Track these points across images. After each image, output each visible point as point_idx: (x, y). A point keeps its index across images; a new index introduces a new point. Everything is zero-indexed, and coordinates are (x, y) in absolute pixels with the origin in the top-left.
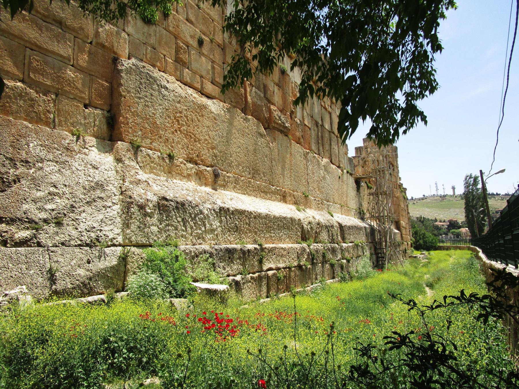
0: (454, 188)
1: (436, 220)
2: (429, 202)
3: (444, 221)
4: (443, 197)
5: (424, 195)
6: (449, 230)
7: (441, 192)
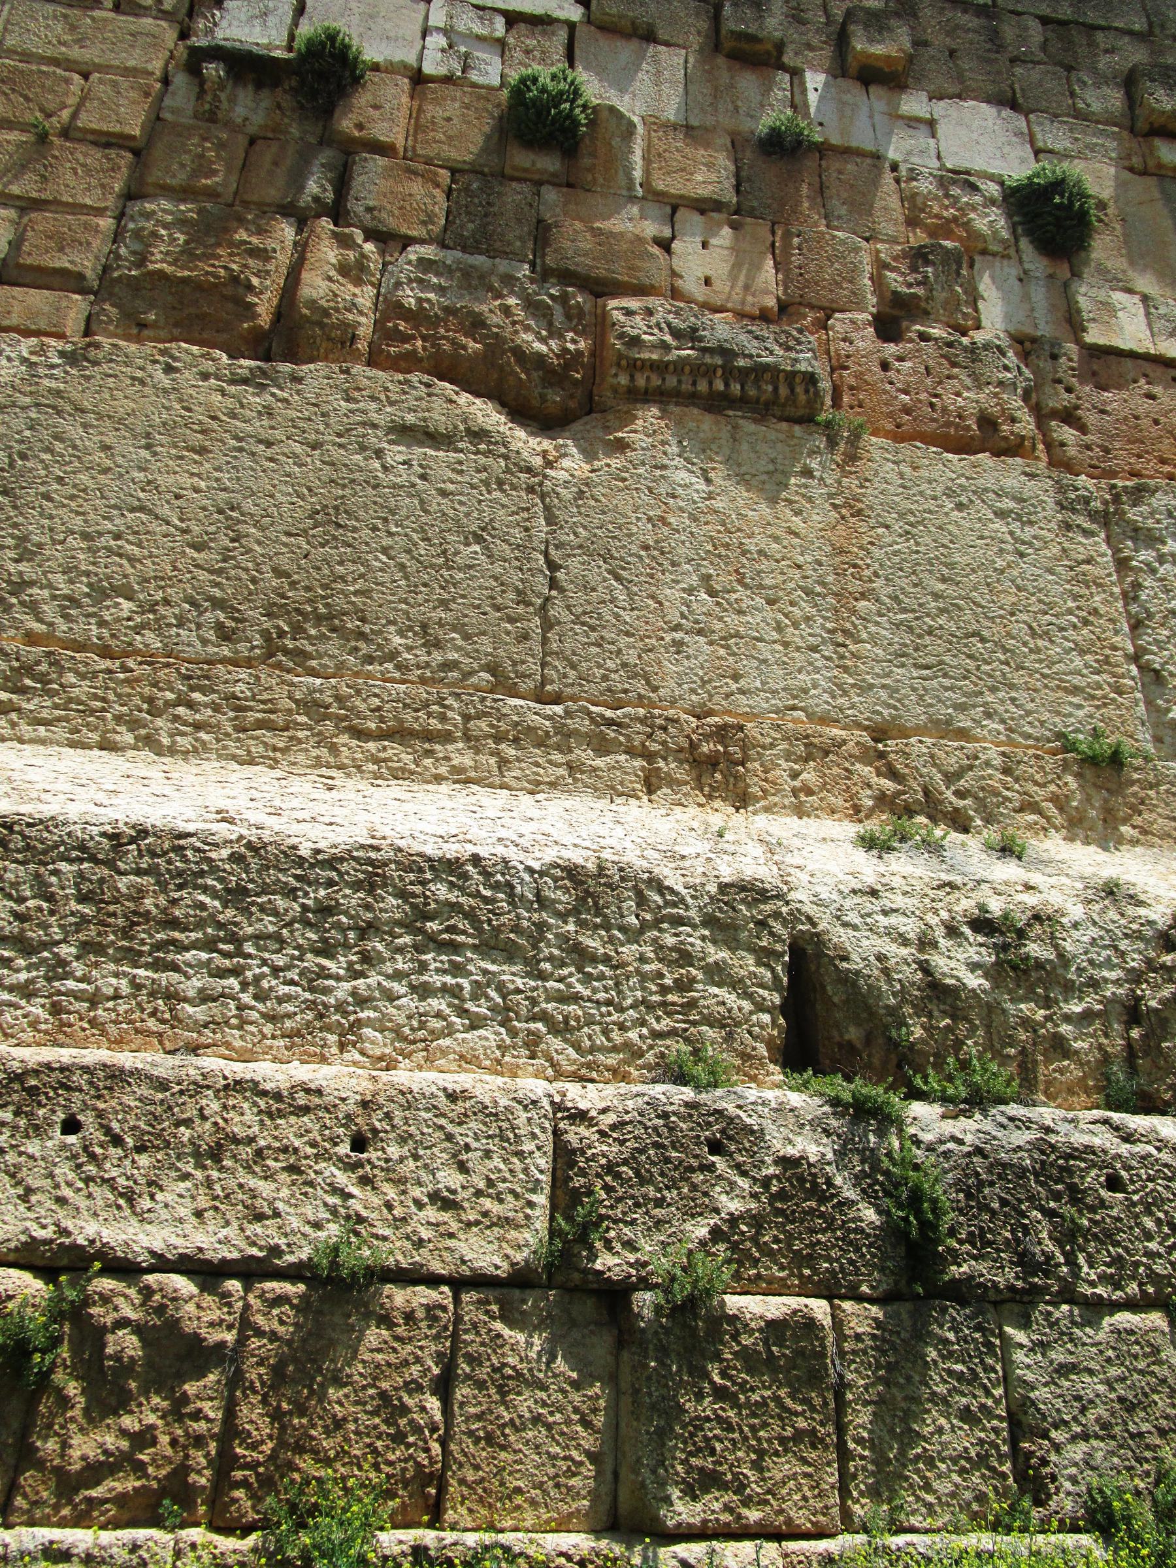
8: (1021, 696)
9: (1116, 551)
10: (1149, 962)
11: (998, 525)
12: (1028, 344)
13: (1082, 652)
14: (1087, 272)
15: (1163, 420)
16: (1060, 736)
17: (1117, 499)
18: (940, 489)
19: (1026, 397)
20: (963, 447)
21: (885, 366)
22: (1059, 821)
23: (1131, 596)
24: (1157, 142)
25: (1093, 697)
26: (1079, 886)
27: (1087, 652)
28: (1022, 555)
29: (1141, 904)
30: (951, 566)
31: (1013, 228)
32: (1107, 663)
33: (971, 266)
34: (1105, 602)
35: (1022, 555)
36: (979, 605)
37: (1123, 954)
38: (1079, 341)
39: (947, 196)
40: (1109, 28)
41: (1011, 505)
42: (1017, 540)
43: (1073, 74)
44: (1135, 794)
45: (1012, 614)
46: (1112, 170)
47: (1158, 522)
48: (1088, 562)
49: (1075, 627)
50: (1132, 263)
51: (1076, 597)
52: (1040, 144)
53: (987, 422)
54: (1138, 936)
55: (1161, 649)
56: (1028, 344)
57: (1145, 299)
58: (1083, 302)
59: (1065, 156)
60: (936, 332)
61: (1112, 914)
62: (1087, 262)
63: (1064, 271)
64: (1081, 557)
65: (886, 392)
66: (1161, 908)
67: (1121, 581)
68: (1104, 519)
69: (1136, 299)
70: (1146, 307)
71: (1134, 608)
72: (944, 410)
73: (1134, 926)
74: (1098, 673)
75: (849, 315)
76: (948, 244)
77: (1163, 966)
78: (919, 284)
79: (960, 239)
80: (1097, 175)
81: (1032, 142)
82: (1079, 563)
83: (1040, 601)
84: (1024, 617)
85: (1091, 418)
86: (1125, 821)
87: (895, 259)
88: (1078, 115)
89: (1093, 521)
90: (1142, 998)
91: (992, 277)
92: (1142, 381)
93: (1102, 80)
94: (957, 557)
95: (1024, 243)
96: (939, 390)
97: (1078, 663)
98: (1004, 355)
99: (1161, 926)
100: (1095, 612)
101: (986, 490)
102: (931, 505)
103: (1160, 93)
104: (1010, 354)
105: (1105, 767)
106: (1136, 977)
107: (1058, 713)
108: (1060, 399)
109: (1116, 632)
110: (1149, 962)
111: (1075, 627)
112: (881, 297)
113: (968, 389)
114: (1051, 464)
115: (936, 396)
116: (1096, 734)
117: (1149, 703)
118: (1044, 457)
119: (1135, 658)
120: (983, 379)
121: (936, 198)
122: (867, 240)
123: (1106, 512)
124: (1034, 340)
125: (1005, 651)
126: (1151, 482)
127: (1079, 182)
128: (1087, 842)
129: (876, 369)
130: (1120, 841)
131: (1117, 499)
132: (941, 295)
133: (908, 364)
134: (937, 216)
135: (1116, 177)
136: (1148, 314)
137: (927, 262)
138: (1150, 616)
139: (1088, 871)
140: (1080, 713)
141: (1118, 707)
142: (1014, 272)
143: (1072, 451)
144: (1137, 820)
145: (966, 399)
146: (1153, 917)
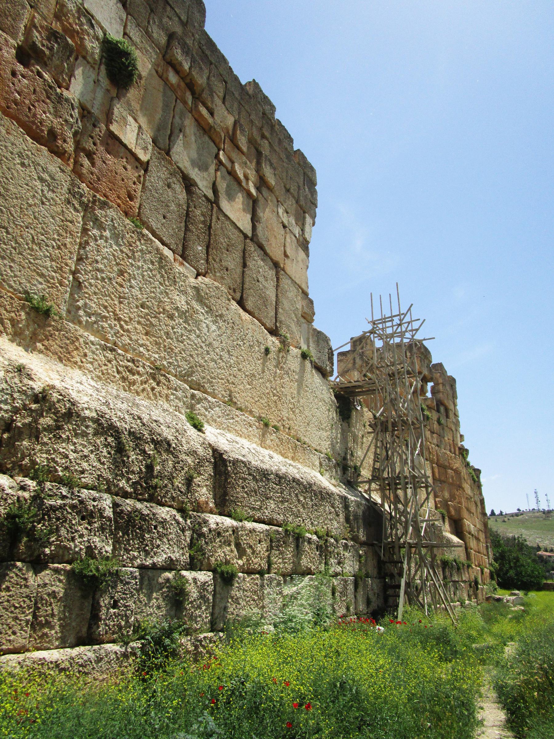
2: (526, 520)
5: (519, 510)
7: (544, 506)
8: (16, 267)
9: (85, 224)
10: (25, 406)
11: (38, 183)
12: (86, 112)
13: (52, 260)
14: (123, 100)
15: (126, 180)
16: (26, 292)
17: (94, 202)
18: (16, 151)
19: (75, 134)
20: (37, 138)
21: (14, 74)
22: (10, 330)
23: (83, 246)
24: (170, 69)
25: (49, 282)
26: (7, 363)
27: (54, 261)
28: (43, 203)
29: (31, 379)
30: (7, 190)
31: (102, 57)
32: (61, 270)
33: (76, 59)
34: (71, 243)
35: (43, 203)
36: (12, 215)
37: (14, 399)
38: (107, 127)
39: (79, 19)
40: (173, 9)
41: (48, 178)
42: (44, 195)
43: (152, 14)
44: (49, 331)
45: (27, 228)
46: (150, 66)
47: (106, 221)
48: (71, 222)
49: (53, 247)
50: (141, 109)
51: (59, 235)
52: (128, 32)
53: (52, 133)
54: (24, 393)
55: (86, 274)
56: (86, 112)
57: (140, 127)
58: (116, 111)
59: (134, 44)
60: (46, 76)
61: (17, 380)
62: (125, 96)
63: (114, 93)
64: (69, 218)
65: (9, 87)
66: (39, 384)
67: (81, 238)
68: (86, 207)
69: (137, 125)
70: (139, 131)
71: (82, 252)
72: (35, 115)
73: (24, 388)
74: (55, 272)
75: (4, 35)
76: (69, 40)
77: (30, 409)
78: (48, 48)
79: (76, 43)
80: (144, 63)
81: (125, 27)
82: (67, 221)
83: (43, 228)
84: (32, 232)
85: (99, 162)
86: (41, 341)
87: (42, 27)
88: (147, 32)
89: (80, 206)
90: (15, 420)
91: (83, 72)
92: (125, 160)
93: (162, 26)
94: (11, 187)
95: (103, 67)
96: (36, 104)
97: (48, 264)
98: (73, 109)
99: (36, 391)
100: (65, 244)
101: (39, 164)
102: (8, 155)
103: (179, 51)
104: (76, 111)
105: (41, 314)
106: (16, 411)
107: (30, 282)
108: (89, 145)
109: (70, 258)
110: (25, 406)
111: (53, 247)
112: (26, 39)
113: (50, 113)
114: (73, 171)
115: (33, 106)
116: (43, 298)
117: (72, 294)
118: (72, 165)
119: (74, 273)
120: (59, 114)
121: (73, 15)
122: (32, 7)
123: (87, 205)
124: (89, 112)
125: (16, 242)
126: (111, 203)
127: (135, 60)
128: (19, 345)
129: (9, 72)
130: (34, 349)
131: (94, 202)
132: (56, 61)
133: (26, 81)
134: (70, 24)
135: (150, 71)
136: (138, 134)
137: (57, 42)
138: (87, 258)
139: (14, 358)
140: (40, 286)
141: (58, 291)
142: (94, 76)
143: (84, 171)
144: (46, 343)
145: (47, 117)
146: (34, 386)
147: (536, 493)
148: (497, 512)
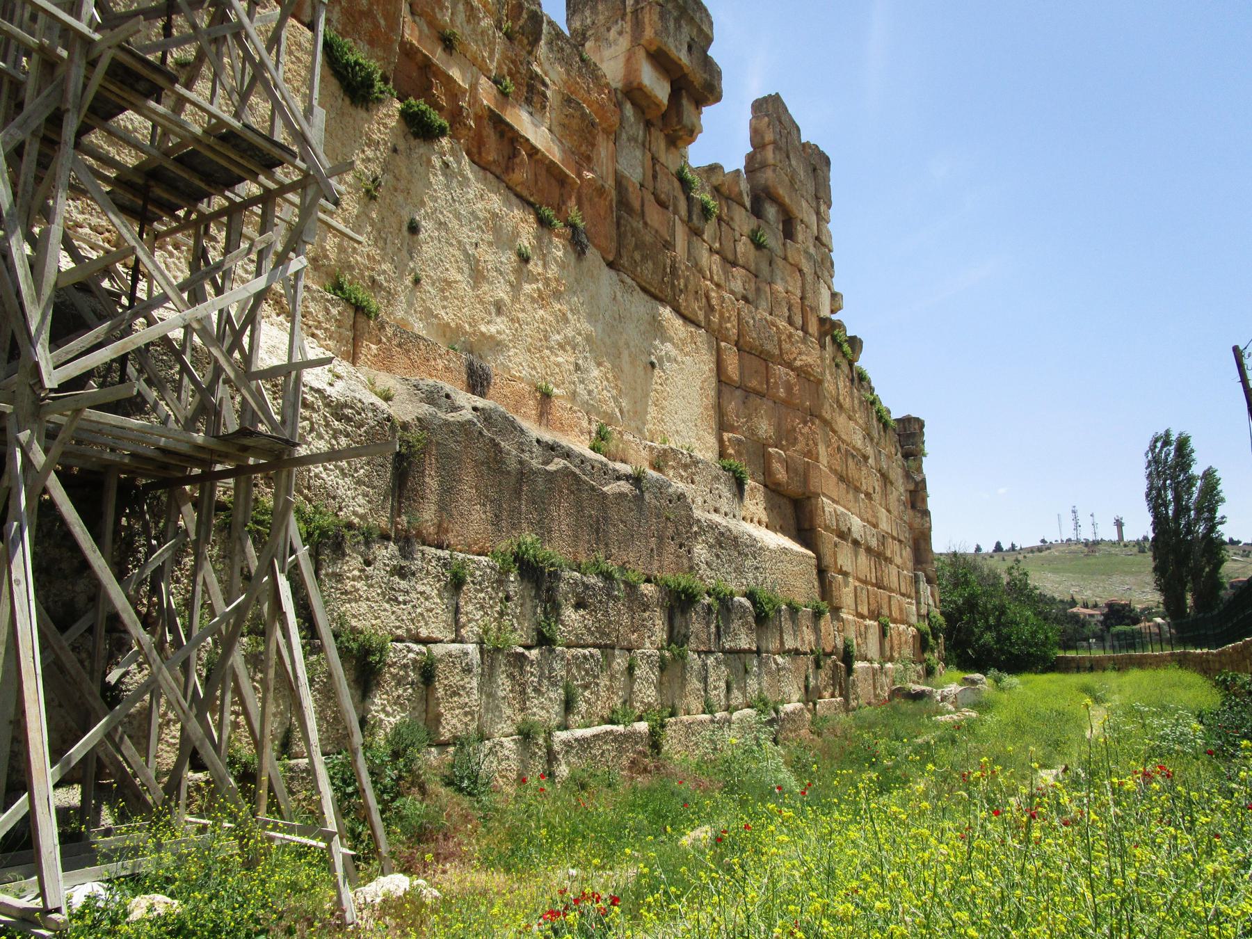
0: (1119, 524)
1: (1073, 603)
2: (1056, 558)
3: (1095, 606)
4: (1093, 546)
6: (1108, 628)
7: (1087, 534)
147: (1074, 512)
148: (1006, 546)
